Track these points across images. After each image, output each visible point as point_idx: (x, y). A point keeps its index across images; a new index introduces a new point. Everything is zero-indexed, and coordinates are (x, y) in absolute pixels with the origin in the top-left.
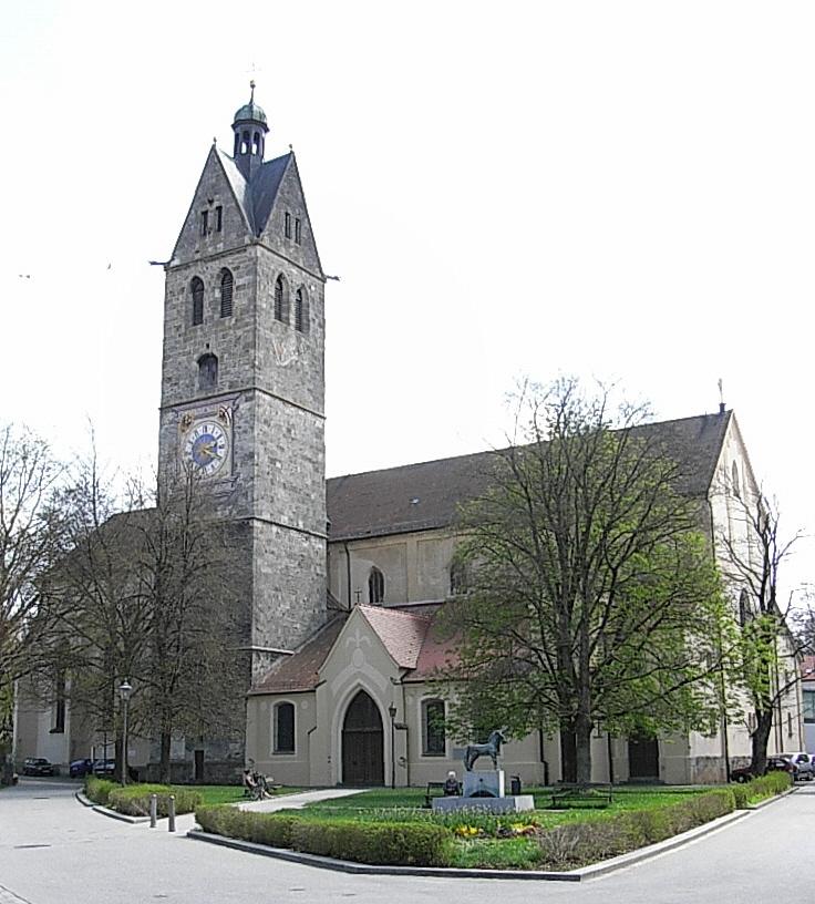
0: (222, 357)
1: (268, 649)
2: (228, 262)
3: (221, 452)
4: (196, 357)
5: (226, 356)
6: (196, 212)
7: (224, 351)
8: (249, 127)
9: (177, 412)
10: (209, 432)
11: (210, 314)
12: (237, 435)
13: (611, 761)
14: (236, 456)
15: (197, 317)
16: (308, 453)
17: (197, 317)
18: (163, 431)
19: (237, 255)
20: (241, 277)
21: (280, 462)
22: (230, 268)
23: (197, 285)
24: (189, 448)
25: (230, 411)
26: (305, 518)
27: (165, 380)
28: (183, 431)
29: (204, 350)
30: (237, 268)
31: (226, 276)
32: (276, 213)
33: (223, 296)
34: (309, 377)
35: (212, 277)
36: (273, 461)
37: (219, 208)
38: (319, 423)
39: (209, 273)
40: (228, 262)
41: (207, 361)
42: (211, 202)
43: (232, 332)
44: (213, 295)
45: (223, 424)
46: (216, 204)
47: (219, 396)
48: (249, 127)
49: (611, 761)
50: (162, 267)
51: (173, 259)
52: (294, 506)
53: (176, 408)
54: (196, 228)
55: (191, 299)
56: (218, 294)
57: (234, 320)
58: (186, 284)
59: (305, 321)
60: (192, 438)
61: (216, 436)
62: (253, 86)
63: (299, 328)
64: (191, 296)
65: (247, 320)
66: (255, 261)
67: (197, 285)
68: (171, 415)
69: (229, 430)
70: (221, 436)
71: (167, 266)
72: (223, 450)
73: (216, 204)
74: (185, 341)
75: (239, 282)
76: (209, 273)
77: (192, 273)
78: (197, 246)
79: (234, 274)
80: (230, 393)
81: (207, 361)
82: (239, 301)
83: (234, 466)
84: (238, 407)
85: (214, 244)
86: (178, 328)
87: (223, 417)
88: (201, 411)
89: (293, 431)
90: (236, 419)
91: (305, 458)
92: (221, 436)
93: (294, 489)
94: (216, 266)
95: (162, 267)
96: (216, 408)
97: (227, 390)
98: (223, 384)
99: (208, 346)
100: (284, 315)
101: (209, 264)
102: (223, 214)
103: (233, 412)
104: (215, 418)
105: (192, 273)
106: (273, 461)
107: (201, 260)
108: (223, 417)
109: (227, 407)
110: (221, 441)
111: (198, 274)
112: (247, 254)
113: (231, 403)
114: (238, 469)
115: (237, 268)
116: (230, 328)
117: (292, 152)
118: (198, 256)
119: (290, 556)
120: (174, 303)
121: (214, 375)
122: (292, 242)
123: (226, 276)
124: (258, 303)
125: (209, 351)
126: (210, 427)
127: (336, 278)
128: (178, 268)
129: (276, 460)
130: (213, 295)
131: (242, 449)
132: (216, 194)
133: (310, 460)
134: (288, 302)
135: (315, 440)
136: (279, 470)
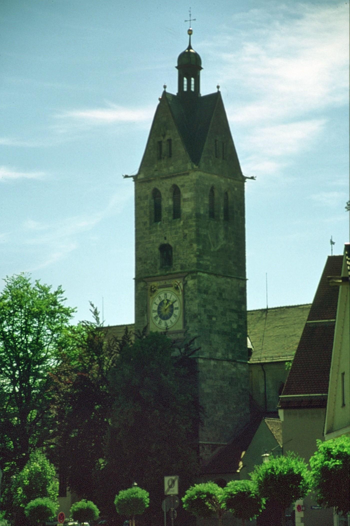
3: (176, 312)
4: (158, 245)
5: (177, 247)
8: (189, 65)
10: (168, 298)
12: (187, 302)
21: (215, 316)
22: (179, 185)
23: (156, 194)
24: (155, 307)
25: (181, 284)
26: (233, 351)
28: (151, 296)
31: (176, 191)
33: (174, 202)
37: (170, 141)
39: (165, 187)
42: (164, 136)
45: (177, 293)
46: (167, 137)
48: (189, 65)
53: (146, 280)
56: (171, 202)
58: (149, 192)
60: (158, 301)
64: (153, 201)
67: (156, 194)
68: (142, 284)
69: (181, 298)
71: (135, 178)
72: (178, 311)
73: (167, 137)
74: (151, 233)
75: (186, 195)
76: (165, 187)
78: (156, 166)
79: (182, 190)
80: (181, 273)
83: (185, 322)
86: (145, 224)
87: (177, 288)
88: (163, 283)
89: (223, 294)
90: (186, 291)
94: (169, 183)
95: (132, 179)
97: (179, 270)
99: (165, 238)
101: (165, 181)
102: (173, 145)
104: (171, 289)
106: (210, 317)
108: (177, 288)
109: (179, 282)
110: (176, 305)
111: (157, 187)
112: (190, 177)
113: (181, 280)
114: (188, 324)
115: (183, 186)
118: (156, 174)
119: (223, 379)
125: (166, 242)
126: (169, 295)
127: (252, 178)
135: (239, 297)
136: (214, 322)
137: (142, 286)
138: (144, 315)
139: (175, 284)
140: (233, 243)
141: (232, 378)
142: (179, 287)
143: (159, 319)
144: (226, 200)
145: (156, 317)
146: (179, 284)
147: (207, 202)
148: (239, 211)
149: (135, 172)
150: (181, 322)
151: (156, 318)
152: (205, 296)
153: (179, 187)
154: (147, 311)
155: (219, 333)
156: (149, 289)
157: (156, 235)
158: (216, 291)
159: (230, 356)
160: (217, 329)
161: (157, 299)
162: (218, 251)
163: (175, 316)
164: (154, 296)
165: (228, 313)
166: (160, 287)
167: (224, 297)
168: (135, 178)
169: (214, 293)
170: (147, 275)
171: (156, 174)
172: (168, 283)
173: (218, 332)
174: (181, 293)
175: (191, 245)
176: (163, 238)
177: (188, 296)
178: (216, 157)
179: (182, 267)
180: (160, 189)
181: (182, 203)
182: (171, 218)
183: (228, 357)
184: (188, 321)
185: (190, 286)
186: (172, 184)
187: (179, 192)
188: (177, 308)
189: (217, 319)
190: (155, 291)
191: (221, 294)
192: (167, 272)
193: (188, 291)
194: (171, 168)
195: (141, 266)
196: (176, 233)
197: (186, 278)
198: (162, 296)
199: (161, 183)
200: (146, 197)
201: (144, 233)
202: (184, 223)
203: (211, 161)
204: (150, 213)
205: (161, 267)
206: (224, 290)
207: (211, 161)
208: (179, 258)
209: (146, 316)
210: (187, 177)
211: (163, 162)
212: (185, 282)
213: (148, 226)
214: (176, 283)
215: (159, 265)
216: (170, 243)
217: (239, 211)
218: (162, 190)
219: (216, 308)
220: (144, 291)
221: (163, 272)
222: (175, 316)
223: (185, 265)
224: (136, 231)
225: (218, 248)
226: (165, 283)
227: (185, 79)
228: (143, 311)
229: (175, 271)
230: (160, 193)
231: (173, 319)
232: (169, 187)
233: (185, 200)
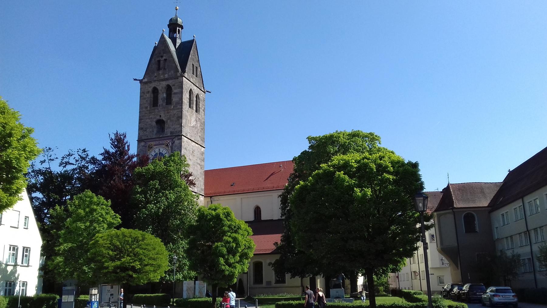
2: (170, 82)
4: (155, 120)
5: (169, 121)
7: (169, 119)
10: (161, 151)
15: (155, 103)
16: (199, 161)
23: (155, 91)
25: (170, 143)
27: (140, 129)
29: (158, 118)
30: (174, 85)
31: (169, 89)
37: (165, 60)
39: (161, 86)
40: (170, 82)
41: (160, 123)
42: (162, 57)
44: (162, 95)
45: (167, 148)
46: (164, 58)
51: (144, 78)
54: (155, 66)
55: (152, 96)
56: (165, 95)
58: (150, 89)
63: (196, 111)
66: (182, 83)
67: (155, 91)
68: (143, 144)
71: (141, 81)
76: (161, 86)
77: (153, 85)
79: (173, 88)
82: (175, 99)
85: (164, 74)
86: (146, 108)
87: (167, 146)
88: (157, 142)
90: (173, 147)
94: (164, 84)
96: (165, 142)
97: (169, 135)
98: (168, 132)
99: (160, 116)
101: (161, 83)
103: (172, 144)
104: (163, 146)
105: (153, 85)
108: (167, 146)
113: (171, 140)
115: (174, 85)
118: (155, 79)
122: (195, 76)
123: (169, 89)
124: (183, 100)
125: (161, 118)
126: (161, 150)
128: (146, 83)
130: (162, 95)
134: (193, 100)
166: (155, 145)
170: (146, 138)
179: (171, 133)
180: (158, 87)
181: (173, 95)
182: (164, 104)
190: (152, 147)
191: (193, 152)
201: (146, 113)
205: (156, 134)
208: (169, 128)
211: (161, 72)
213: (149, 109)
215: (155, 132)
216: (164, 119)
218: (159, 88)
233: (175, 93)
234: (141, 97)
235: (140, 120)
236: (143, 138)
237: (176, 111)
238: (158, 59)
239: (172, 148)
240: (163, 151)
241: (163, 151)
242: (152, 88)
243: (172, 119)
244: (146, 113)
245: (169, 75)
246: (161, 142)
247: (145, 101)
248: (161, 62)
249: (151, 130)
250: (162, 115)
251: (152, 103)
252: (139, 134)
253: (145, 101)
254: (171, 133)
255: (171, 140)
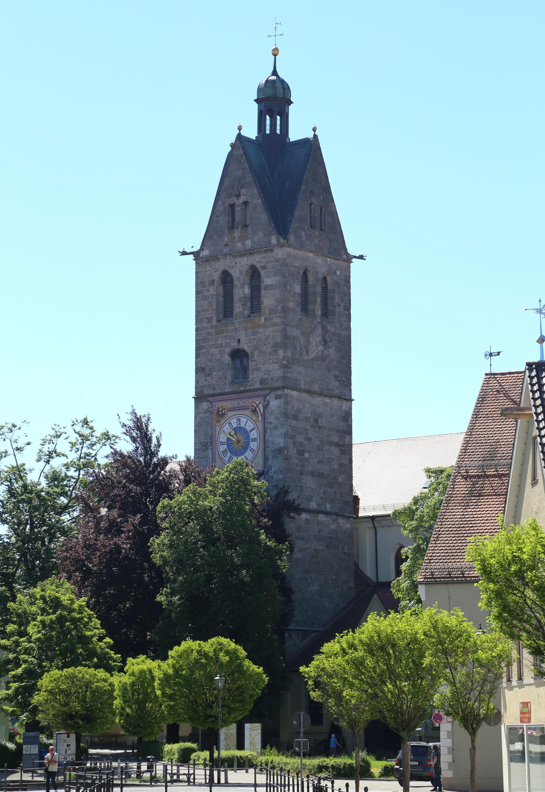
0: (254, 353)
1: (299, 628)
2: (257, 260)
3: (254, 445)
4: (228, 350)
5: (256, 353)
6: (224, 203)
8: (274, 99)
9: (211, 402)
10: (242, 425)
11: (241, 310)
13: (473, 761)
14: (268, 450)
15: (227, 310)
17: (227, 310)
18: (198, 419)
19: (265, 255)
20: (268, 277)
21: (308, 452)
22: (258, 266)
23: (226, 278)
25: (261, 406)
27: (199, 370)
28: (218, 421)
29: (234, 345)
30: (264, 267)
31: (254, 274)
32: (301, 211)
33: (252, 290)
34: (335, 363)
35: (241, 273)
36: (301, 453)
37: (246, 203)
38: (345, 405)
39: (239, 268)
40: (257, 260)
41: (238, 355)
42: (238, 196)
43: (261, 330)
44: (241, 291)
45: (255, 418)
46: (243, 198)
47: (247, 391)
48: (274, 99)
49: (473, 761)
50: (192, 257)
51: (202, 249)
52: (322, 491)
53: (210, 399)
54: (224, 220)
55: (221, 291)
56: (247, 291)
57: (263, 318)
58: (216, 276)
59: (330, 307)
60: (227, 428)
61: (249, 429)
62: (275, 55)
63: (325, 314)
64: (221, 288)
65: (275, 320)
67: (226, 278)
68: (205, 405)
69: (260, 425)
70: (253, 429)
71: (196, 255)
72: (255, 443)
73: (243, 198)
75: (267, 281)
76: (239, 268)
77: (222, 265)
79: (262, 273)
81: (238, 355)
83: (266, 459)
84: (269, 403)
85: (243, 239)
86: (210, 320)
87: (254, 411)
88: (234, 404)
89: (320, 421)
90: (267, 415)
91: (332, 444)
92: (253, 429)
93: (321, 475)
94: (245, 262)
95: (192, 257)
96: (248, 402)
97: (257, 386)
98: (255, 378)
99: (239, 341)
100: (310, 307)
101: (238, 260)
103: (265, 407)
104: (247, 412)
105: (222, 265)
106: (301, 453)
107: (230, 255)
108: (254, 411)
110: (254, 435)
111: (228, 269)
112: (273, 254)
113: (261, 399)
115: (264, 267)
116: (259, 326)
117: (315, 136)
118: (226, 250)
120: (205, 294)
121: (245, 369)
123: (254, 274)
125: (241, 346)
126: (243, 420)
127: (361, 257)
128: (207, 260)
129: (304, 451)
130: (241, 291)
131: (273, 443)
132: (242, 188)
133: (337, 445)
137: (205, 408)
138: (207, 449)
139: (253, 406)
140: (333, 349)
141: (330, 537)
142: (257, 409)
143: (229, 454)
144: (325, 289)
145: (225, 451)
146: (257, 406)
147: (298, 289)
148: (342, 304)
149: (197, 248)
150: (260, 459)
151: (224, 452)
152: (295, 422)
153: (259, 269)
154: (211, 443)
155: (313, 476)
156: (215, 412)
157: (226, 336)
158: (309, 415)
159: (329, 507)
160: (311, 469)
161: (227, 426)
162: (313, 359)
163: (252, 450)
164: (222, 422)
165: (326, 447)
167: (320, 424)
168: (196, 255)
169: (307, 419)
170: (211, 392)
171: (226, 250)
172: (242, 403)
173: (312, 474)
174: (260, 418)
175: (276, 351)
176: (236, 340)
177: (271, 423)
178: (312, 227)
179: (262, 381)
180: (231, 271)
181: (263, 292)
183: (325, 508)
184: (270, 458)
185: (273, 408)
186: (249, 264)
187: (259, 276)
188: (254, 440)
189: (310, 455)
190: (223, 415)
192: (241, 388)
193: (271, 415)
194: (249, 243)
195: (204, 379)
196: (254, 334)
197: (268, 397)
198: (234, 422)
199: (234, 263)
200: (213, 282)
201: (209, 334)
202: (265, 319)
203: (303, 234)
204: (217, 304)
205: (233, 382)
206: (320, 415)
207: (303, 234)
208: (258, 369)
209: (210, 450)
210: (271, 255)
211: (237, 234)
212: (266, 403)
213: (214, 322)
214: (254, 404)
215: (229, 378)
217: (342, 304)
218: (235, 273)
219: (309, 440)
220: (208, 415)
221: (235, 388)
222: (252, 450)
223: (267, 379)
224: (197, 330)
225: (312, 356)
226: (238, 404)
227: (268, 117)
228: (207, 443)
229: (253, 387)
230: (231, 277)
231: (249, 454)
232: (245, 268)
233: (267, 287)
234: (198, 293)
235: (198, 348)
236: (206, 392)
237: (270, 329)
238: (229, 201)
239: (264, 416)
240: (247, 423)
241: (247, 423)
242: (219, 273)
243: (264, 349)
244: (209, 334)
245: (253, 242)
246: (242, 403)
247: (206, 303)
248: (237, 208)
249: (221, 373)
250: (243, 338)
251: (222, 307)
252: (197, 382)
253: (206, 303)
254: (262, 381)
255: (261, 399)
